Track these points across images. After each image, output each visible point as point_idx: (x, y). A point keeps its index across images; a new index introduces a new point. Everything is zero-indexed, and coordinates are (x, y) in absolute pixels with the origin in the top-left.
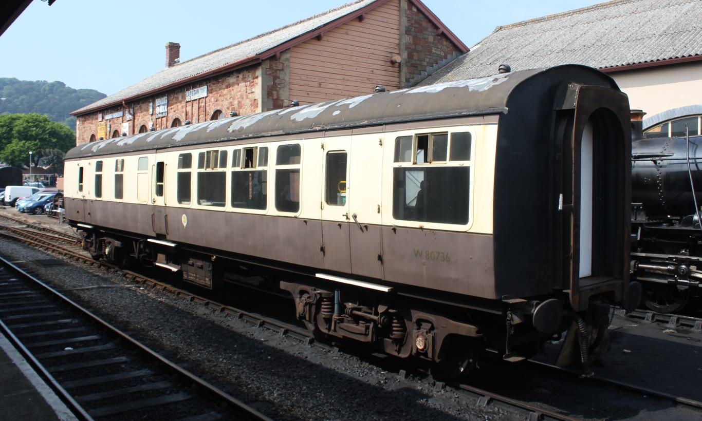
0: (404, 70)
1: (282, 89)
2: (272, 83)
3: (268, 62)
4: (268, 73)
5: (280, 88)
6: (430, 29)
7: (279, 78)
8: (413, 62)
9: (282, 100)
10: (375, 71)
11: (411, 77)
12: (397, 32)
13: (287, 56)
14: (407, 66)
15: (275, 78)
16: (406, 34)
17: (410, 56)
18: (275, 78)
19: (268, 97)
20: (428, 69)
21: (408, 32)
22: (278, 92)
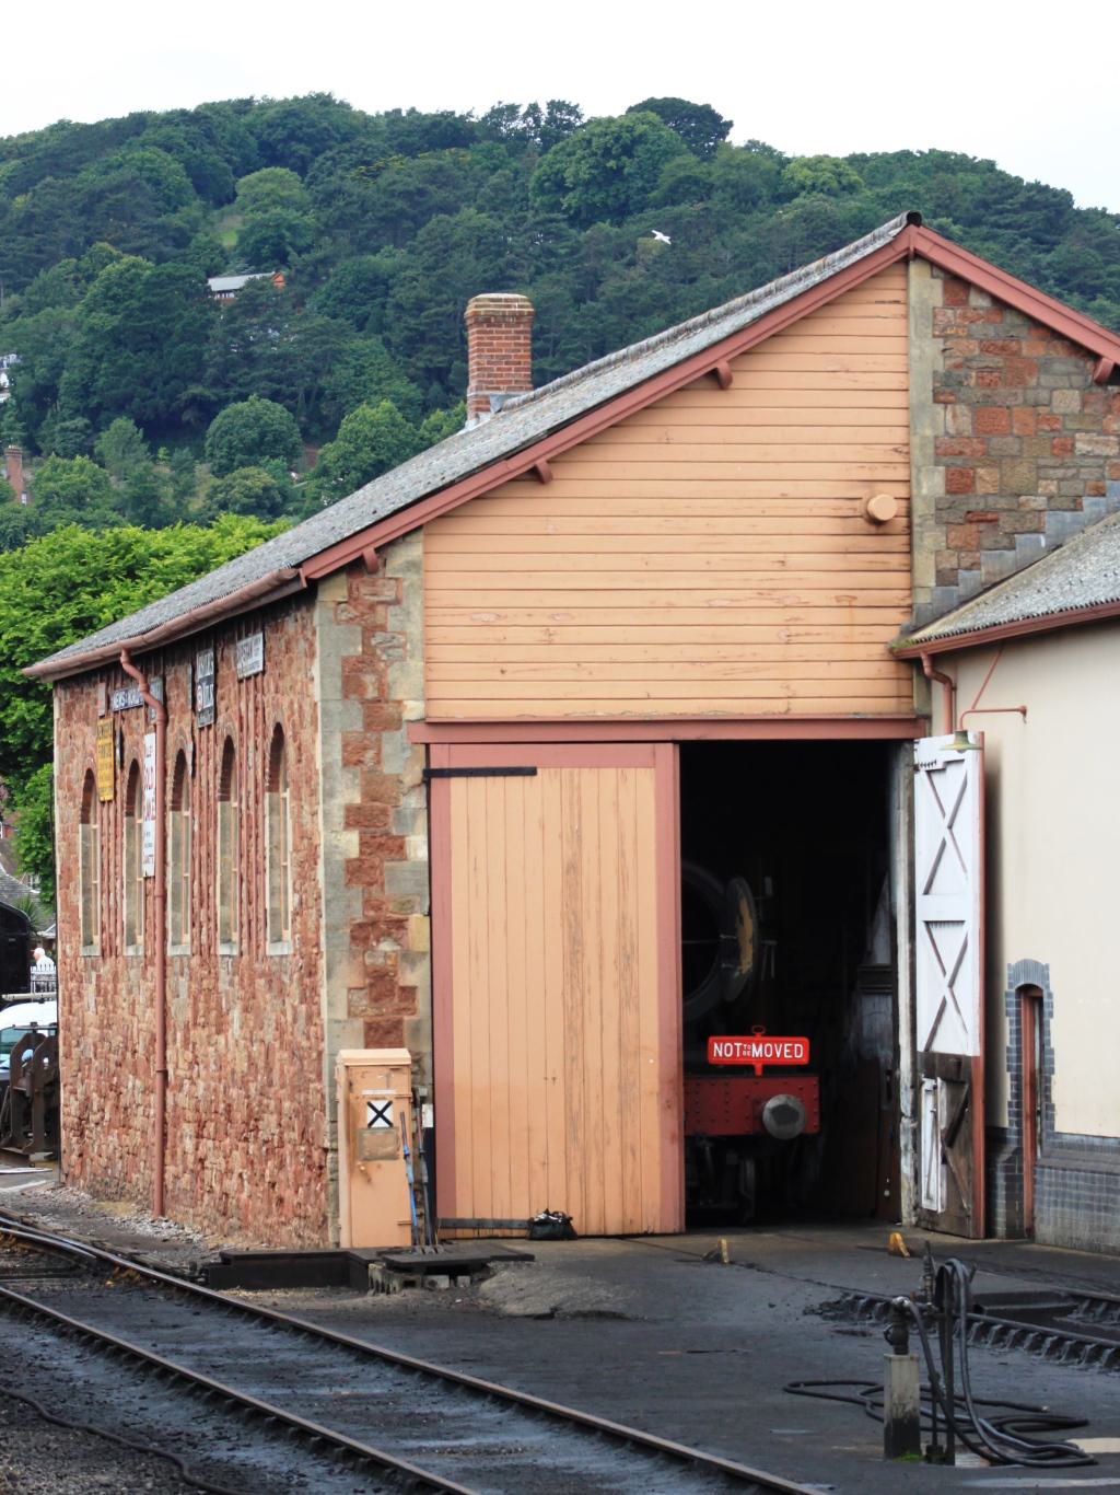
0: (930, 540)
1: (396, 665)
2: (360, 649)
3: (342, 579)
4: (343, 617)
5: (389, 664)
6: (1064, 363)
7: (383, 628)
8: (975, 504)
9: (399, 702)
10: (792, 559)
11: (966, 562)
12: (898, 399)
13: (413, 551)
14: (939, 521)
15: (369, 631)
16: (936, 401)
17: (959, 484)
18: (369, 631)
19: (346, 696)
20: (1051, 521)
21: (946, 390)
22: (381, 676)
